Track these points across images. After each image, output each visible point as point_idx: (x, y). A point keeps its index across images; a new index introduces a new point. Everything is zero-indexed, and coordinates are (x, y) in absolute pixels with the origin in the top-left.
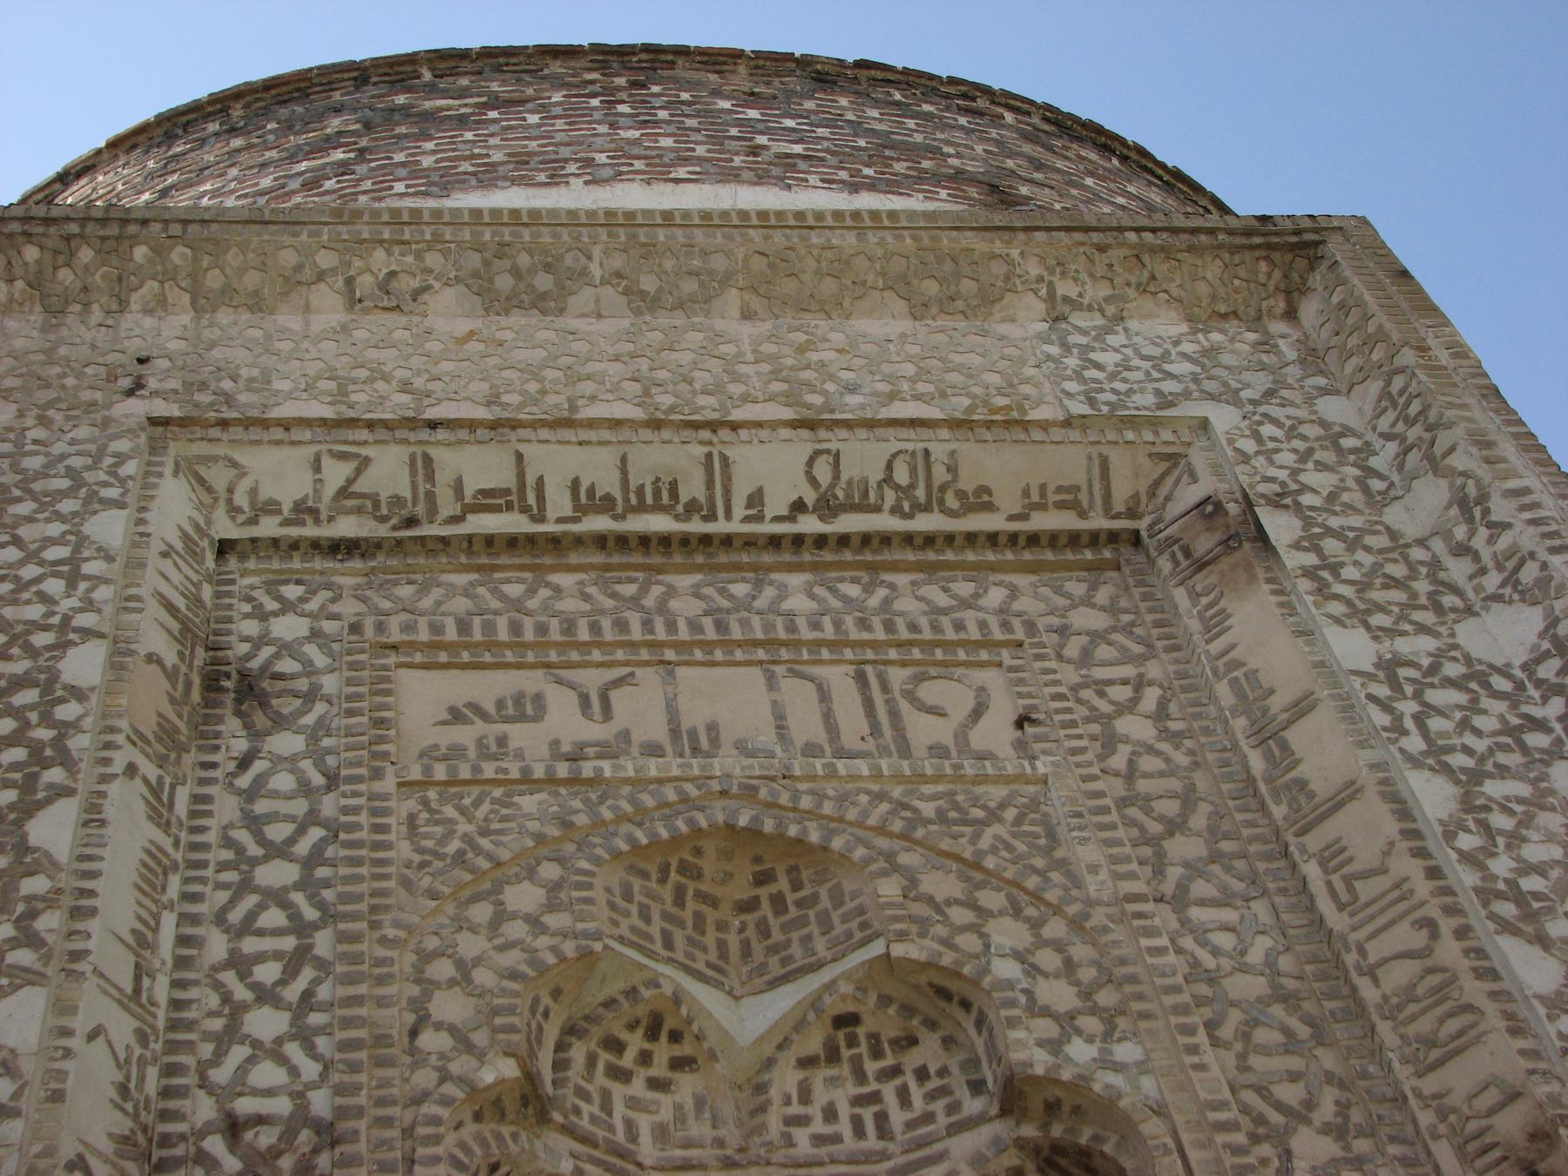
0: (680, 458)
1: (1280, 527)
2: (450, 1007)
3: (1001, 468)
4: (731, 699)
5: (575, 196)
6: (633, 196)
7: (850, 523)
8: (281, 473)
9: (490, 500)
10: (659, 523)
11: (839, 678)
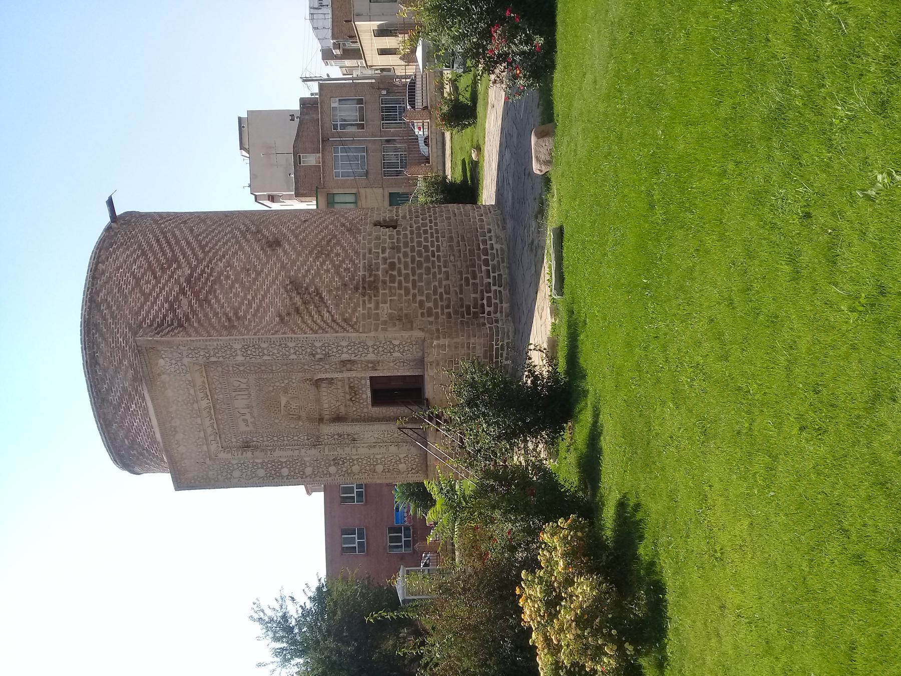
0: (205, 414)
1: (213, 359)
2: (293, 426)
3: (199, 381)
4: (240, 403)
5: (157, 430)
6: (154, 422)
7: (208, 393)
8: (213, 447)
9: (213, 427)
10: (212, 411)
11: (234, 394)
